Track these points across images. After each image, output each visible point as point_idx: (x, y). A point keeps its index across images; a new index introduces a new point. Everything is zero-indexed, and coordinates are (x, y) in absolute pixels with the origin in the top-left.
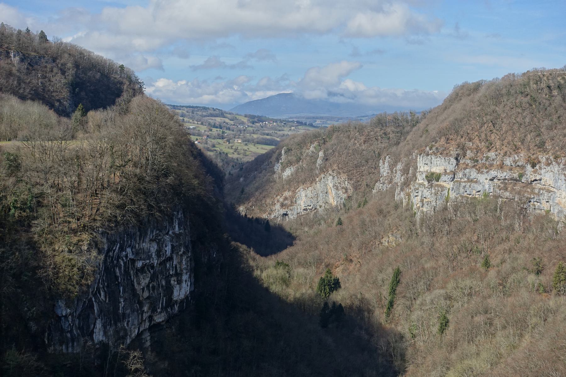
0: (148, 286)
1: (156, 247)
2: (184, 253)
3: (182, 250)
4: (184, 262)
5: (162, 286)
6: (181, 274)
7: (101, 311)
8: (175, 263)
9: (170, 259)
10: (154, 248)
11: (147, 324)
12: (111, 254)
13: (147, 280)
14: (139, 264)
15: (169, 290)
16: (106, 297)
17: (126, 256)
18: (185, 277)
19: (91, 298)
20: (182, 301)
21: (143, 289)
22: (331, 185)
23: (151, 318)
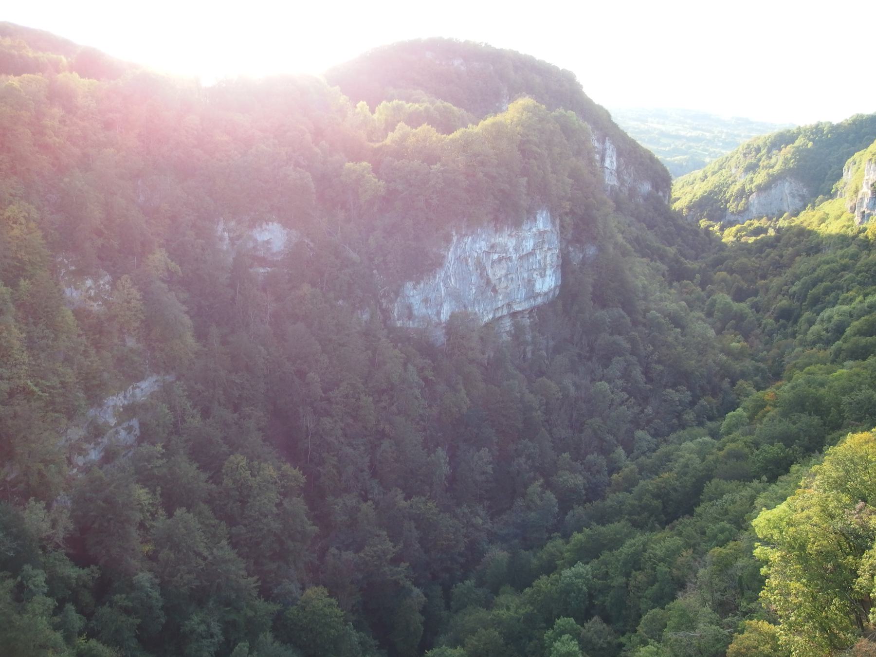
0: (506, 275)
1: (514, 242)
2: (549, 249)
3: (546, 247)
4: (548, 259)
5: (523, 279)
6: (545, 270)
7: (448, 294)
8: (538, 258)
9: (532, 253)
10: (511, 243)
11: (505, 312)
12: (462, 245)
13: (504, 272)
14: (496, 256)
15: (530, 283)
16: (456, 283)
17: (480, 248)
18: (549, 272)
19: (438, 284)
20: (546, 294)
21: (500, 279)
22: (787, 192)
23: (509, 305)
